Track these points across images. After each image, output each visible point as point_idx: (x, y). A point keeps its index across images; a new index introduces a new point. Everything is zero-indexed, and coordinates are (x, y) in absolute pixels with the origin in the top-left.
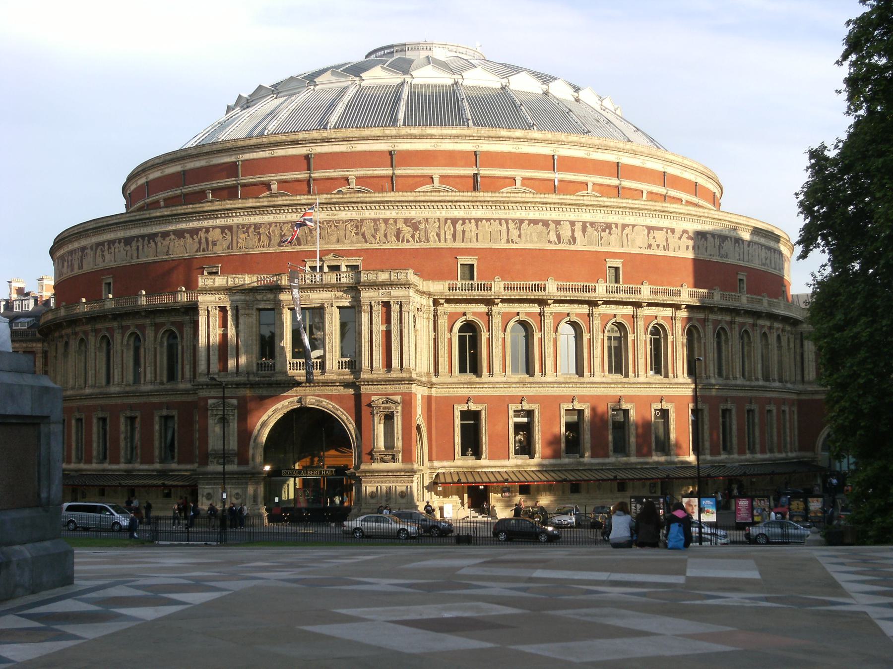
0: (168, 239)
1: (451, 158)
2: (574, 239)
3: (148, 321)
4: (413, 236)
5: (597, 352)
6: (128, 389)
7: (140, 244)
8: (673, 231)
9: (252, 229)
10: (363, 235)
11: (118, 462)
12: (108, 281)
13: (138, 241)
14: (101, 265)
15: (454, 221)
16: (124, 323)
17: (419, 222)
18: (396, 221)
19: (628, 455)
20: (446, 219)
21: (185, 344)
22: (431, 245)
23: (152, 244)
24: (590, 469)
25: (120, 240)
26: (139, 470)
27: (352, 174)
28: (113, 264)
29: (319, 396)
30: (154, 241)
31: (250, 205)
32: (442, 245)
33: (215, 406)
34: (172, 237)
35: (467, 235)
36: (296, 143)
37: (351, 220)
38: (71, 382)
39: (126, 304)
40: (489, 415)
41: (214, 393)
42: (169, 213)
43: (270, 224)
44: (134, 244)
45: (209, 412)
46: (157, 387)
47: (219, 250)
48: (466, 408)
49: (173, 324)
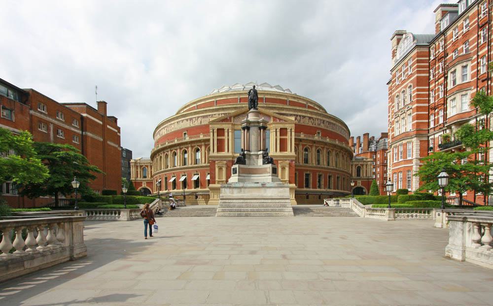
3: (190, 145)
16: (181, 147)
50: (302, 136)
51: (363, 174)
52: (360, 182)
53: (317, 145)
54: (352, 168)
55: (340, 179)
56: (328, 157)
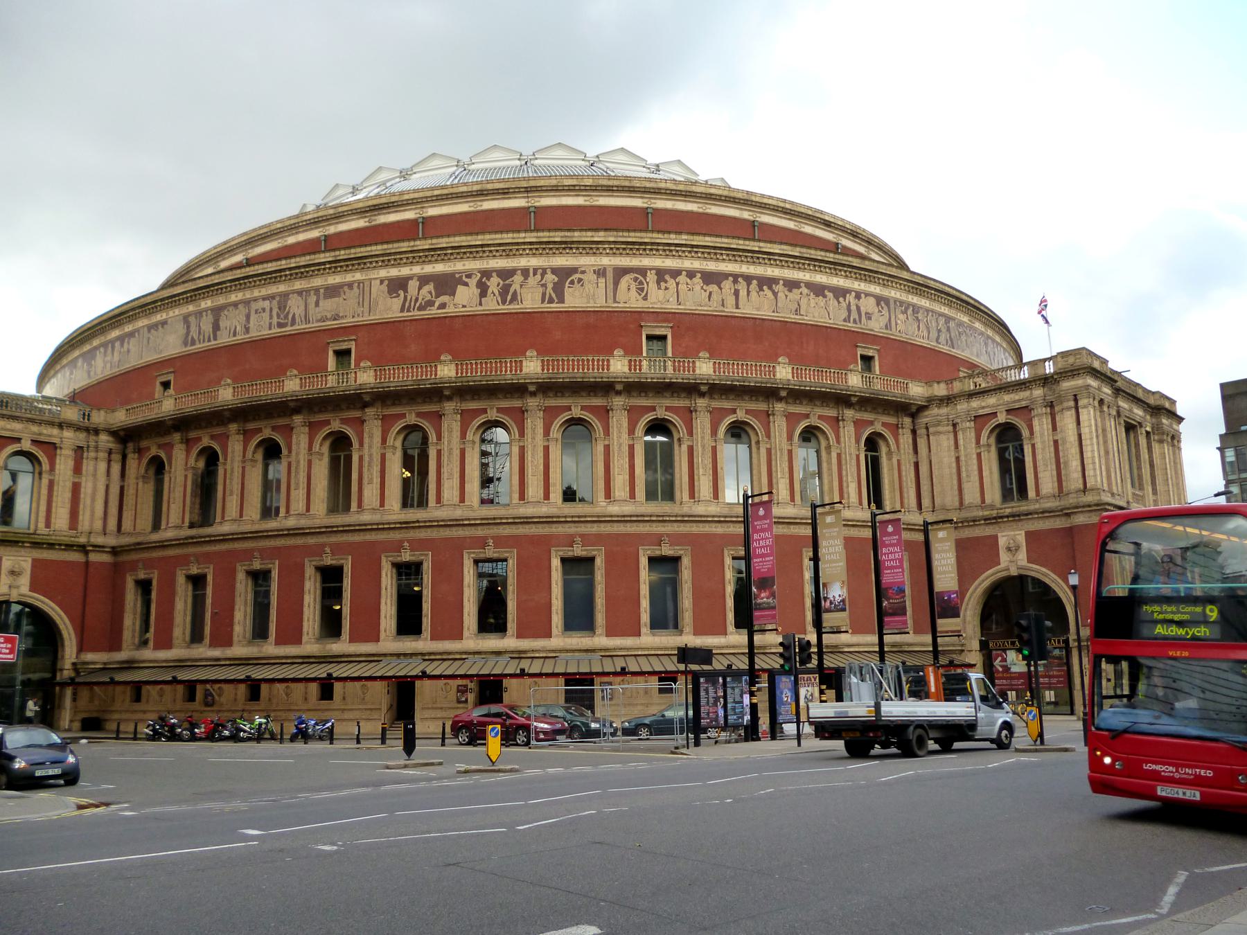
0: (795, 291)
9: (910, 311)
12: (658, 332)
13: (735, 281)
23: (769, 294)
25: (691, 274)
28: (672, 306)
30: (770, 288)
34: (805, 291)
43: (927, 311)
44: (727, 285)
47: (876, 325)
49: (820, 417)
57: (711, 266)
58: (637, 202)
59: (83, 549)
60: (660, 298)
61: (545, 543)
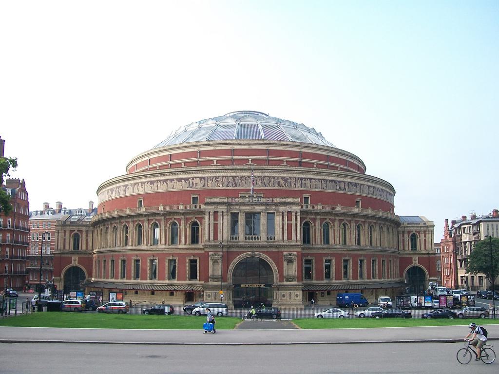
1: (291, 154)
2: (345, 189)
3: (163, 218)
4: (285, 185)
5: (353, 236)
6: (152, 247)
7: (159, 184)
8: (375, 187)
10: (264, 183)
11: (146, 279)
13: (157, 182)
14: (136, 192)
15: (302, 179)
16: (149, 219)
17: (288, 179)
18: (278, 178)
19: (363, 279)
20: (299, 178)
21: (181, 228)
22: (293, 188)
24: (352, 285)
26: (158, 283)
27: (250, 158)
28: (143, 192)
29: (259, 252)
31: (214, 168)
32: (297, 189)
33: (213, 255)
34: (175, 181)
35: (307, 185)
36: (226, 144)
37: (259, 177)
38: (118, 243)
39: (153, 210)
40: (316, 262)
41: (211, 250)
42: (174, 171)
43: (223, 177)
44: (155, 184)
45: (210, 258)
46: (167, 247)
47: (199, 187)
48: (307, 258)
50: (320, 207)
51: (421, 249)
52: (417, 258)
53: (341, 218)
54: (403, 236)
55: (377, 263)
56: (359, 231)
57: (152, 179)
58: (167, 153)
59: (87, 254)
60: (141, 190)
61: (118, 256)
